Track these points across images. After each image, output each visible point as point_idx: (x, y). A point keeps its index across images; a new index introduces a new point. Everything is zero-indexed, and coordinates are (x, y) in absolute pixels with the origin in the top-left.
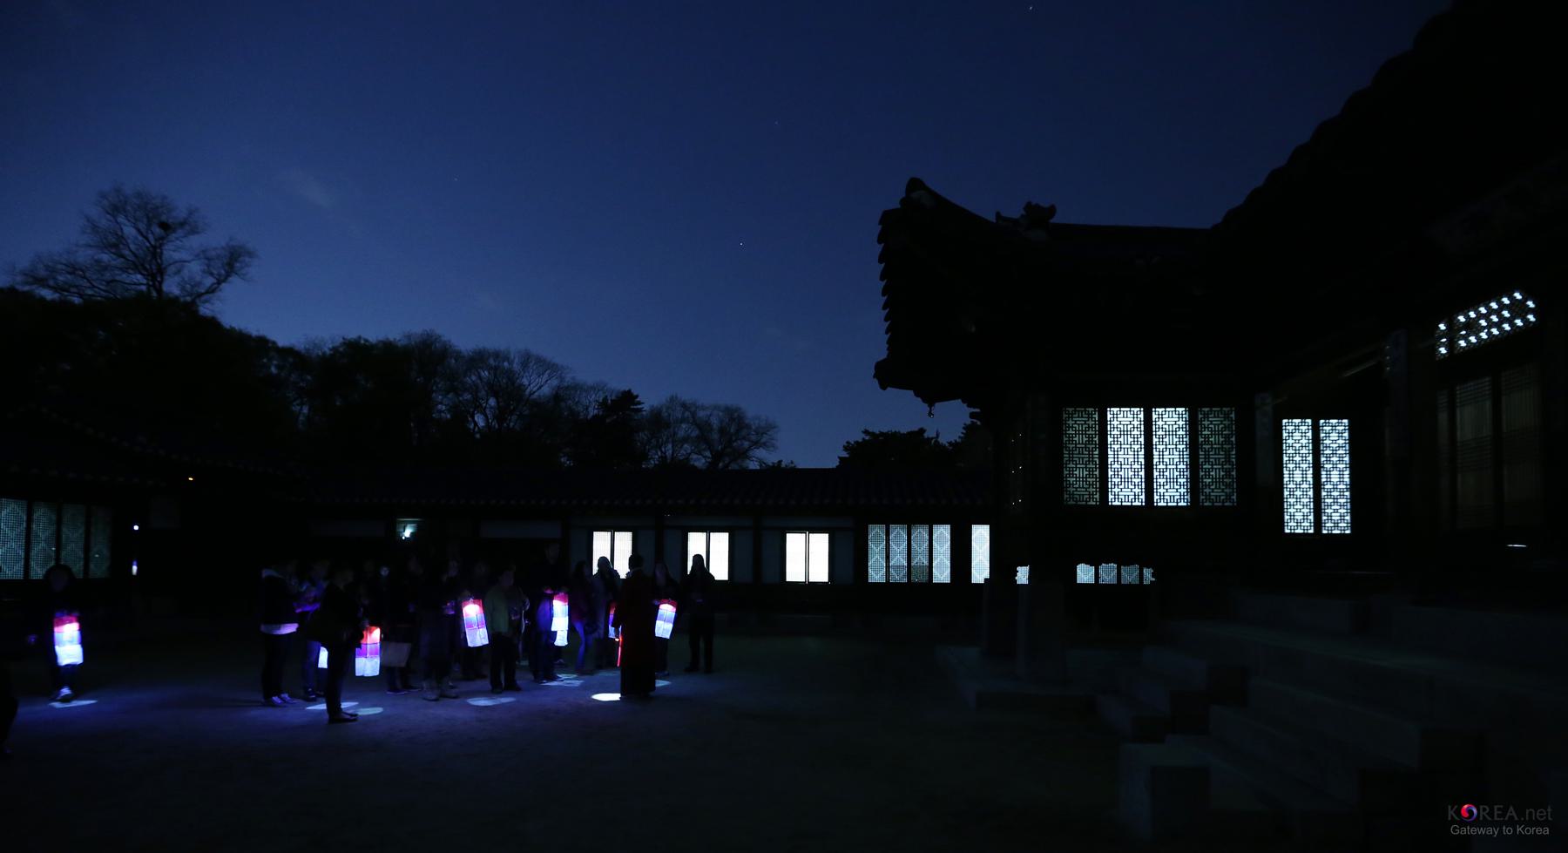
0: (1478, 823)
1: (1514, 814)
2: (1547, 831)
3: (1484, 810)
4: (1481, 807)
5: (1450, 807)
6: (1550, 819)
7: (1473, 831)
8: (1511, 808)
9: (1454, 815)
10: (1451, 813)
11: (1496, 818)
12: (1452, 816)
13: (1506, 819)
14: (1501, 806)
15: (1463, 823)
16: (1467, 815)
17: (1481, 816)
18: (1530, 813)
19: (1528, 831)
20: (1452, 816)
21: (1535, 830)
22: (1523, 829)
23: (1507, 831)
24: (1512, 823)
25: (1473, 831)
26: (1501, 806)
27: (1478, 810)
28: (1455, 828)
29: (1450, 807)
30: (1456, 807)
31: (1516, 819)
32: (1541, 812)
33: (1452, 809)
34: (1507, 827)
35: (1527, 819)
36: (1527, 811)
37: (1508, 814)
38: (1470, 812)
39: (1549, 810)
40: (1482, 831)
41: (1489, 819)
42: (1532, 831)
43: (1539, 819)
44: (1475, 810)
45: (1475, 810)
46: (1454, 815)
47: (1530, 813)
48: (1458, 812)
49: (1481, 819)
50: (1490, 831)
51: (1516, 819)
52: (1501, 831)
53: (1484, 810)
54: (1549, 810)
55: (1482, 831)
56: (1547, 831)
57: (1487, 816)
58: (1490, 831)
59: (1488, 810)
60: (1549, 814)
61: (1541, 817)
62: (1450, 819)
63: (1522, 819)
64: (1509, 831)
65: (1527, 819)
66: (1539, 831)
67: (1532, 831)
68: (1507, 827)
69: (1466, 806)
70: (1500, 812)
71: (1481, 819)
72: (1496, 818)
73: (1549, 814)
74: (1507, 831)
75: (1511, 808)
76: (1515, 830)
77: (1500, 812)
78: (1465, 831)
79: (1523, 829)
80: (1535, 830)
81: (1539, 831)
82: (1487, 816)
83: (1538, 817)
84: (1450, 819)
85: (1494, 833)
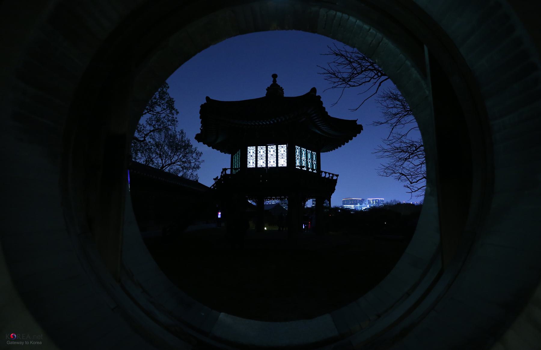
0: (16, 340)
2: (41, 343)
3: (19, 335)
4: (18, 335)
7: (15, 343)
8: (28, 335)
9: (8, 338)
12: (7, 338)
15: (11, 340)
16: (13, 338)
19: (34, 343)
20: (7, 338)
22: (32, 342)
23: (27, 343)
25: (15, 343)
27: (17, 336)
33: (7, 335)
40: (18, 343)
44: (15, 336)
45: (15, 336)
46: (8, 338)
48: (10, 336)
49: (18, 338)
50: (21, 343)
52: (25, 343)
55: (18, 343)
56: (41, 343)
58: (21, 343)
61: (39, 338)
63: (32, 339)
64: (28, 343)
66: (38, 343)
69: (12, 334)
70: (24, 336)
71: (18, 338)
74: (27, 343)
75: (28, 335)
76: (30, 343)
77: (24, 336)
78: (12, 343)
79: (32, 342)
81: (38, 343)
85: (22, 344)
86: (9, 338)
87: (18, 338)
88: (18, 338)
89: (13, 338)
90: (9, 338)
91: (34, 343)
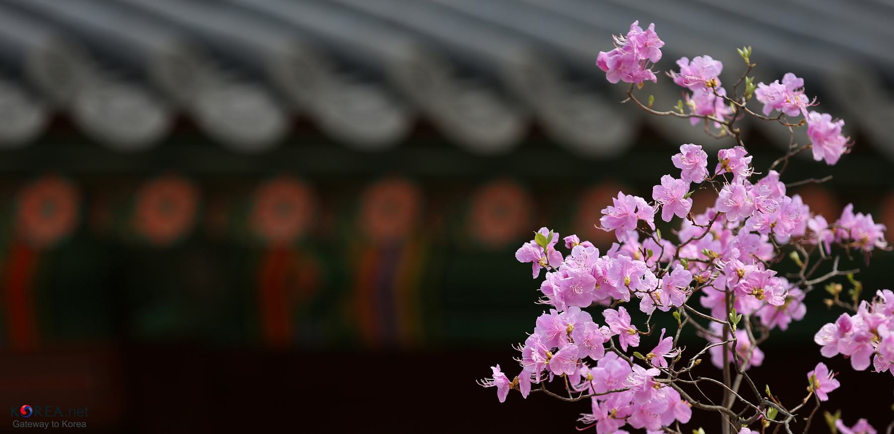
0: (33, 418)
7: (29, 425)
15: (22, 419)
19: (70, 425)
21: (75, 424)
23: (54, 424)
28: (16, 423)
31: (62, 416)
40: (36, 425)
41: (41, 415)
42: (73, 424)
44: (31, 410)
45: (31, 410)
51: (62, 416)
52: (50, 424)
64: (57, 425)
66: (78, 425)
67: (73, 424)
69: (24, 406)
70: (49, 411)
76: (61, 424)
77: (49, 411)
78: (23, 425)
79: (67, 423)
80: (75, 424)
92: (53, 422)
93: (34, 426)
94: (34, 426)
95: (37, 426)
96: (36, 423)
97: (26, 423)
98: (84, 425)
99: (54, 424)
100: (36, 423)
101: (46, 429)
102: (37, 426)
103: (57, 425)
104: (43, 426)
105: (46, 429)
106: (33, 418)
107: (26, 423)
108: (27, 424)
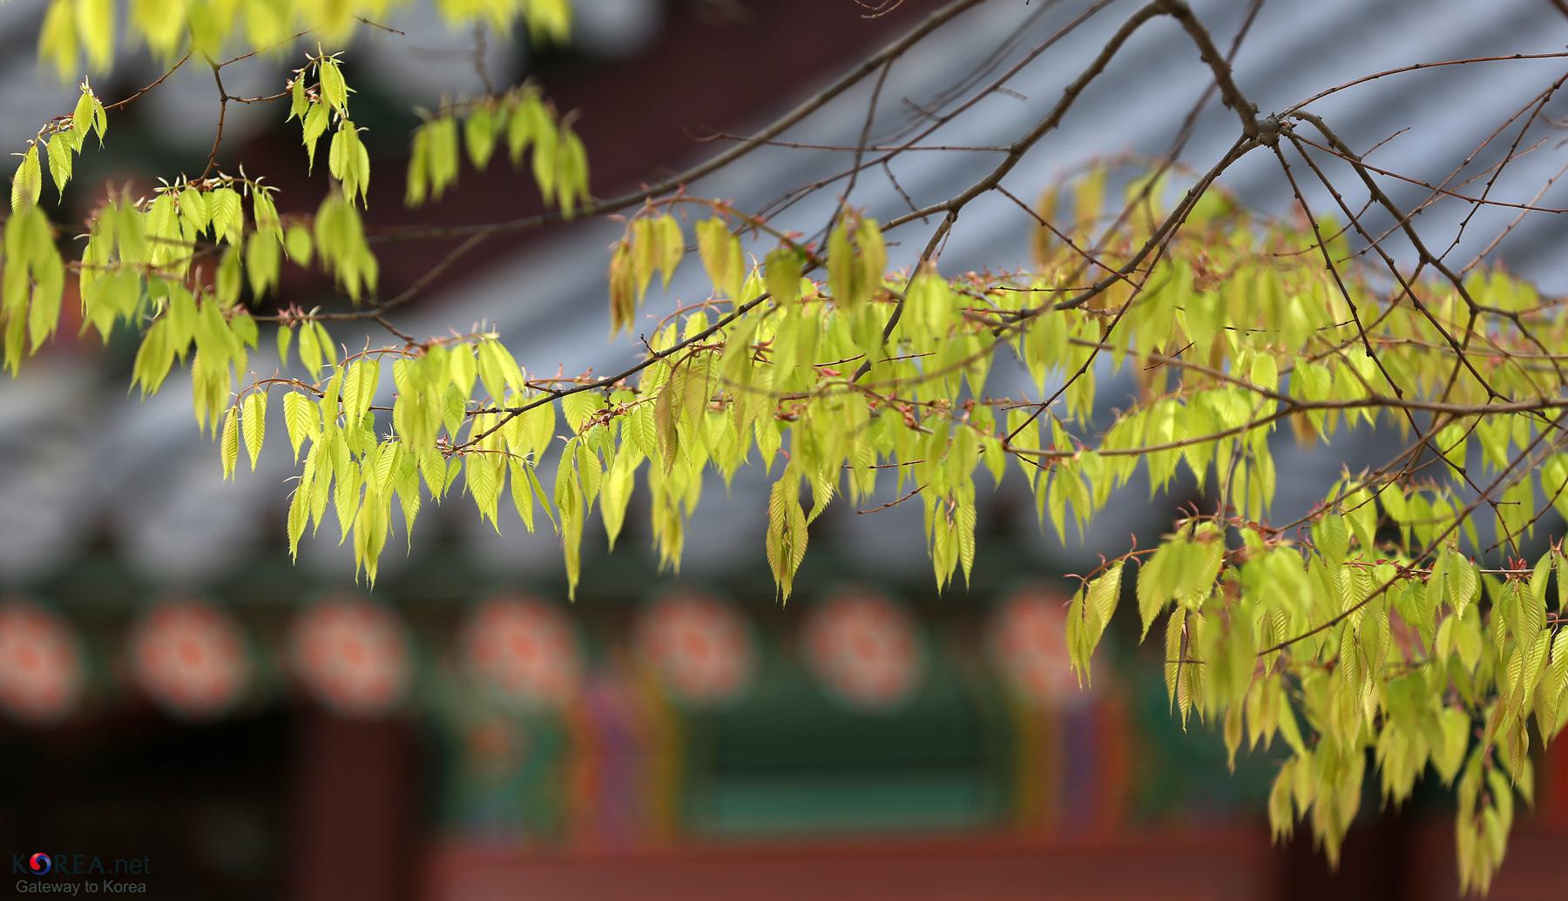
0: (50, 878)
1: (100, 866)
2: (143, 888)
3: (61, 860)
5: (15, 857)
6: (147, 872)
7: (45, 888)
8: (96, 859)
10: (16, 864)
11: (75, 872)
13: (90, 871)
14: (83, 856)
15: (32, 878)
16: (36, 867)
17: (56, 866)
18: (121, 865)
19: (118, 888)
20: (18, 870)
21: (127, 887)
22: (112, 886)
23: (90, 887)
24: (97, 878)
25: (45, 888)
26: (83, 856)
28: (24, 884)
29: (15, 857)
30: (23, 856)
31: (103, 872)
32: (136, 863)
34: (90, 883)
35: (117, 871)
36: (117, 862)
37: (93, 865)
38: (42, 863)
39: (146, 860)
40: (57, 888)
43: (133, 872)
44: (48, 862)
45: (48, 862)
46: (21, 867)
47: (121, 865)
49: (57, 872)
50: (68, 888)
51: (103, 872)
52: (82, 889)
53: (61, 860)
54: (146, 860)
55: (57, 888)
57: (64, 869)
58: (68, 888)
59: (65, 859)
60: (146, 864)
61: (136, 869)
62: (15, 872)
64: (94, 888)
65: (117, 871)
67: (123, 887)
68: (90, 883)
69: (36, 856)
70: (81, 863)
71: (57, 872)
72: (75, 872)
73: (146, 864)
74: (90, 887)
76: (101, 887)
77: (81, 863)
78: (34, 888)
79: (112, 886)
80: (127, 887)
81: (133, 888)
82: (64, 869)
83: (131, 870)
84: (15, 872)
86: (24, 871)
87: (60, 868)
88: (60, 868)
89: (41, 870)
90: (24, 871)
91: (118, 889)
92: (87, 884)
93: (54, 891)
94: (54, 891)
95: (59, 891)
96: (57, 885)
97: (40, 884)
98: (143, 888)
99: (89, 886)
100: (57, 885)
101: (74, 895)
102: (59, 891)
103: (94, 888)
104: (70, 890)
105: (74, 895)
106: (50, 878)
107: (40, 884)
108: (42, 886)
